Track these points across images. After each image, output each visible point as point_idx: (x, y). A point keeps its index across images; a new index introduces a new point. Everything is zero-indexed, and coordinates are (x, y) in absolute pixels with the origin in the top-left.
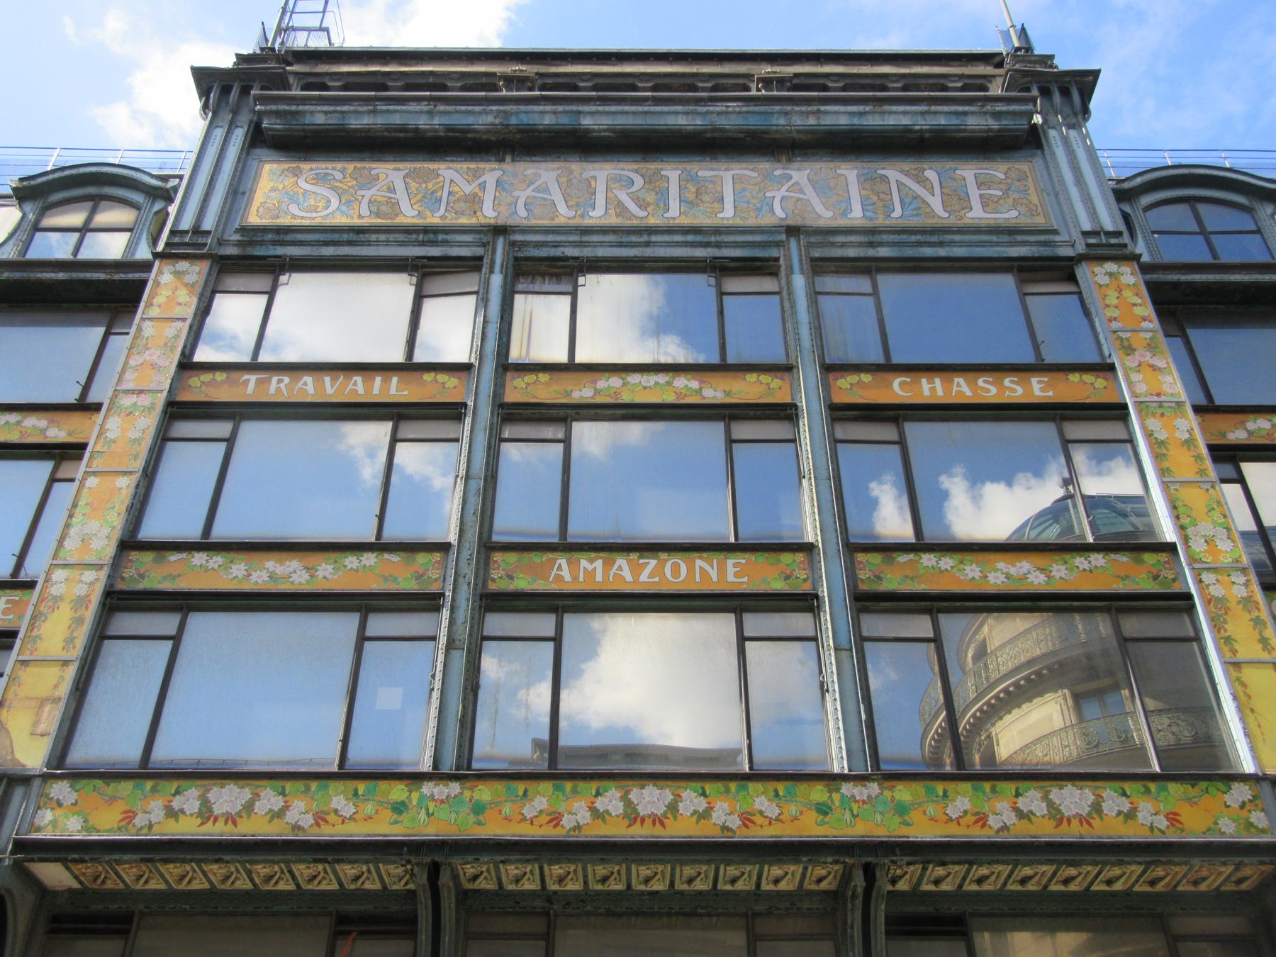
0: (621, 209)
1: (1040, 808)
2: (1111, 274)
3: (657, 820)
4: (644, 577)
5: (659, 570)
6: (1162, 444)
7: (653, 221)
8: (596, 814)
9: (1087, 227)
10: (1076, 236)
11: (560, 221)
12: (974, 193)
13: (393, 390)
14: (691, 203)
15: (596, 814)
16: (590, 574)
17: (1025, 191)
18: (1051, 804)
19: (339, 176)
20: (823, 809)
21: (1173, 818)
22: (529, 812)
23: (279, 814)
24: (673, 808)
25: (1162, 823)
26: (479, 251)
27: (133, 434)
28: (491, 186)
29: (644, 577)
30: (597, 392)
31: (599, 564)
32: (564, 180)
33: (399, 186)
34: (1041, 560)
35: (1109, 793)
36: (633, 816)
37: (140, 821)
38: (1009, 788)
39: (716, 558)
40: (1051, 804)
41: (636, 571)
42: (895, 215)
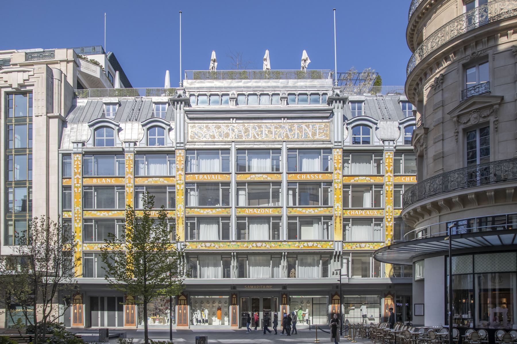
0: (255, 137)
1: (306, 245)
2: (337, 152)
3: (260, 247)
4: (258, 212)
5: (260, 211)
6: (336, 189)
7: (260, 139)
8: (253, 246)
9: (336, 140)
10: (333, 142)
11: (244, 139)
12: (318, 131)
13: (219, 178)
14: (267, 134)
15: (253, 246)
16: (251, 212)
17: (327, 131)
18: (308, 245)
19: (203, 127)
20: (280, 245)
21: (322, 246)
22: (244, 246)
23: (214, 246)
24: (262, 245)
25: (320, 247)
26: (230, 146)
27: (182, 188)
28: (231, 129)
29: (258, 212)
30: (251, 178)
31: (252, 210)
32: (244, 128)
33: (214, 130)
34: (314, 209)
35: (315, 243)
36: (257, 246)
37: (198, 247)
38: (303, 243)
39: (268, 209)
40: (308, 245)
41: (257, 211)
42: (303, 137)
